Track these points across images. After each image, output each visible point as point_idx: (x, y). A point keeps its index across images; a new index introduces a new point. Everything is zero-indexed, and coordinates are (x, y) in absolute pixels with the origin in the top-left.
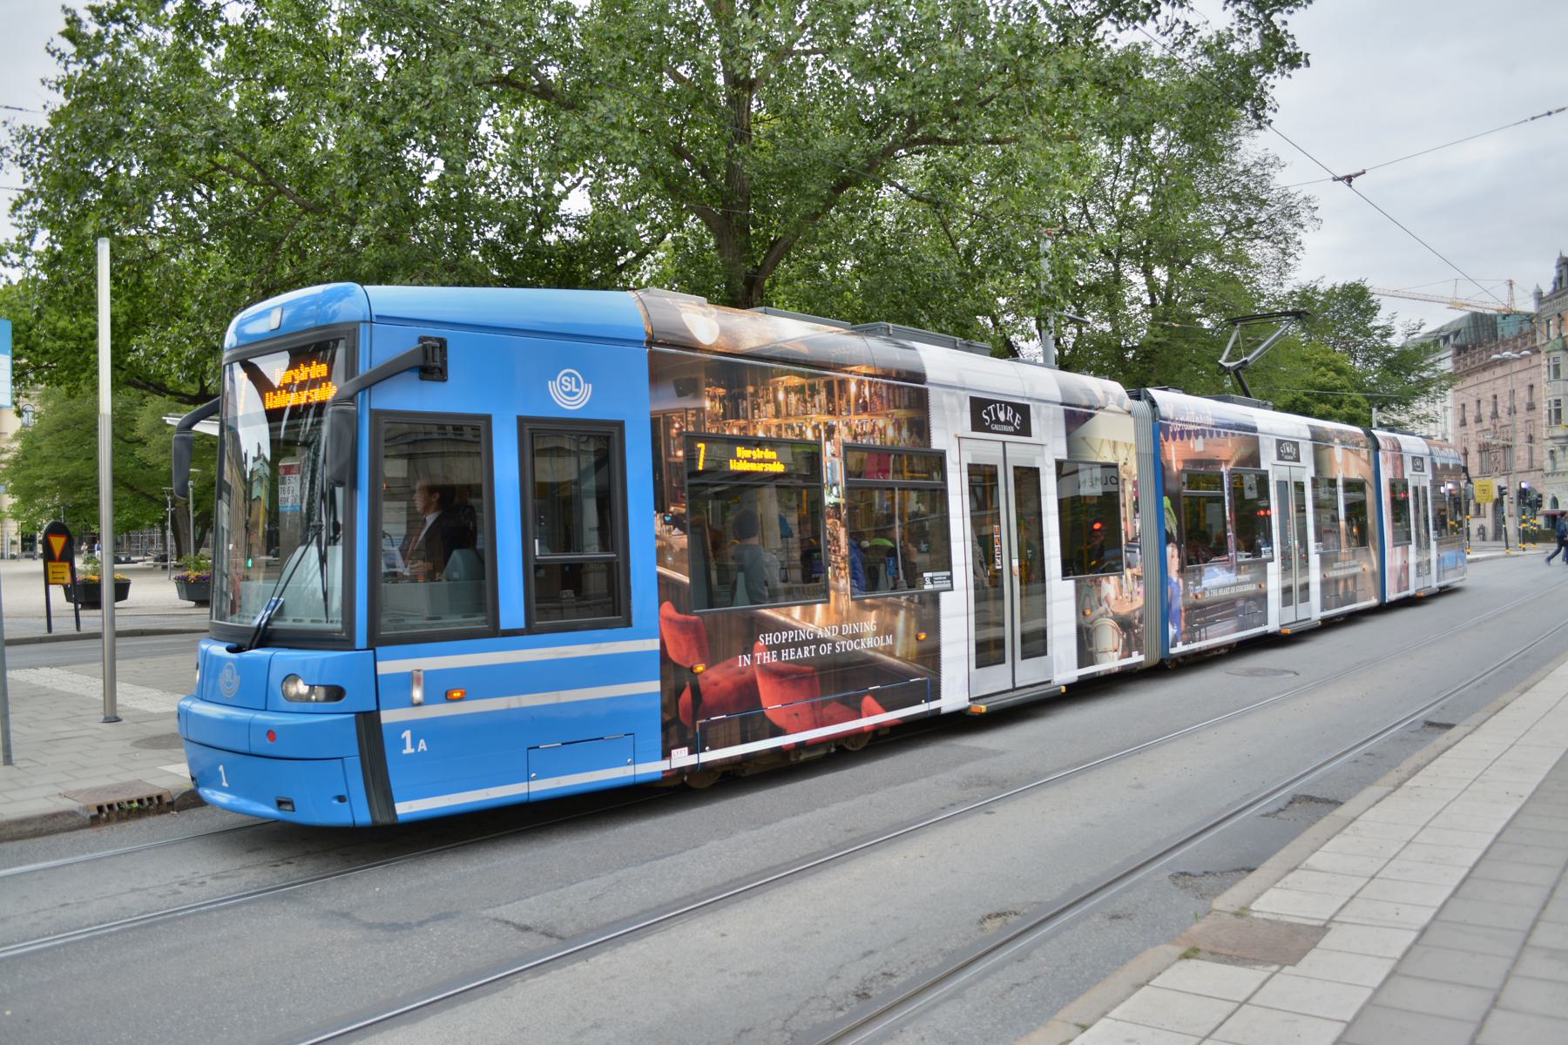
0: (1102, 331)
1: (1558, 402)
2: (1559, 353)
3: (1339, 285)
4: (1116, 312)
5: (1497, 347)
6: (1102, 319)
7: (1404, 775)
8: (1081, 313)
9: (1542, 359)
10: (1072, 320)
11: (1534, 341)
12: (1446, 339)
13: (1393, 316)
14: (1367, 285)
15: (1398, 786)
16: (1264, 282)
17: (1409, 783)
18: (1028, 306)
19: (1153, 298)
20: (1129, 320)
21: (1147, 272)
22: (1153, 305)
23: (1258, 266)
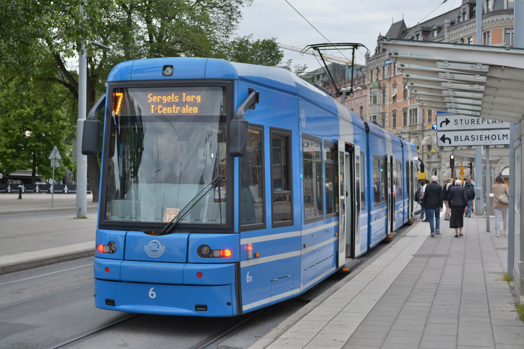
0: (118, 55)
1: (375, 117)
2: (376, 90)
3: (261, 40)
4: (128, 44)
5: (345, 83)
6: (119, 48)
7: (280, 331)
8: (106, 43)
9: (367, 92)
10: (100, 47)
11: (364, 82)
12: (318, 77)
13: (290, 61)
14: (277, 41)
15: (276, 339)
16: (218, 34)
17: (282, 336)
18: (69, 35)
19: (151, 37)
20: (136, 49)
21: (149, 22)
22: (151, 41)
23: (215, 24)
